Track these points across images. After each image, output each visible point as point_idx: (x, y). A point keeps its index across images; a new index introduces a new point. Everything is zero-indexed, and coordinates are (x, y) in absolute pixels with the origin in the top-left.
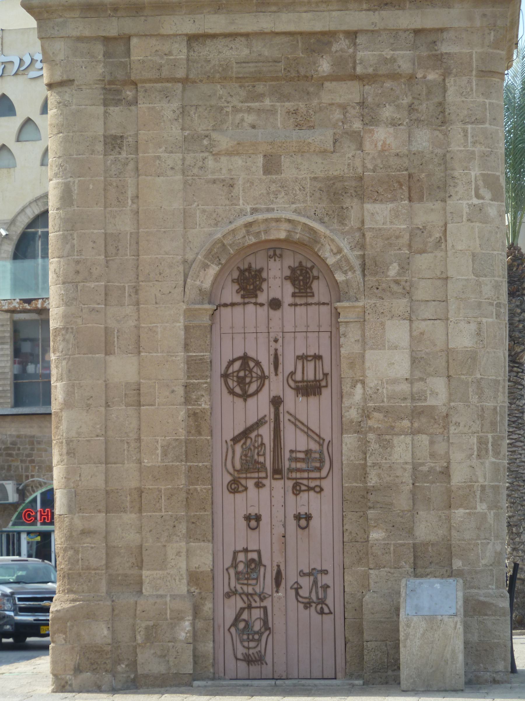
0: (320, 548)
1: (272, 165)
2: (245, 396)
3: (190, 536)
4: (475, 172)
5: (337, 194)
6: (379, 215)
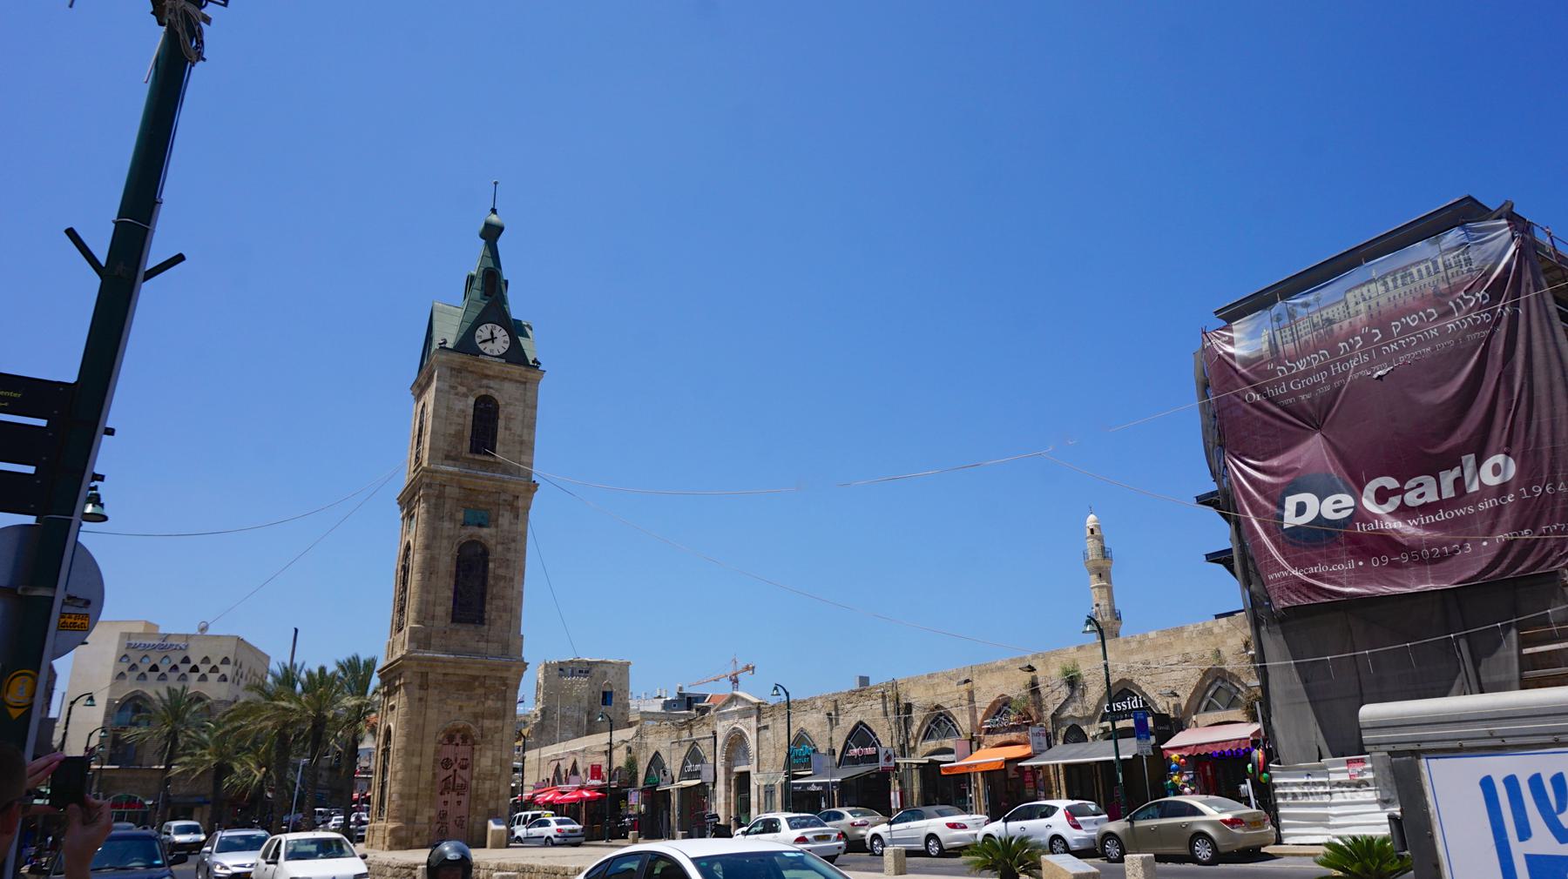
0: (463, 810)
1: (461, 708)
6: (487, 723)
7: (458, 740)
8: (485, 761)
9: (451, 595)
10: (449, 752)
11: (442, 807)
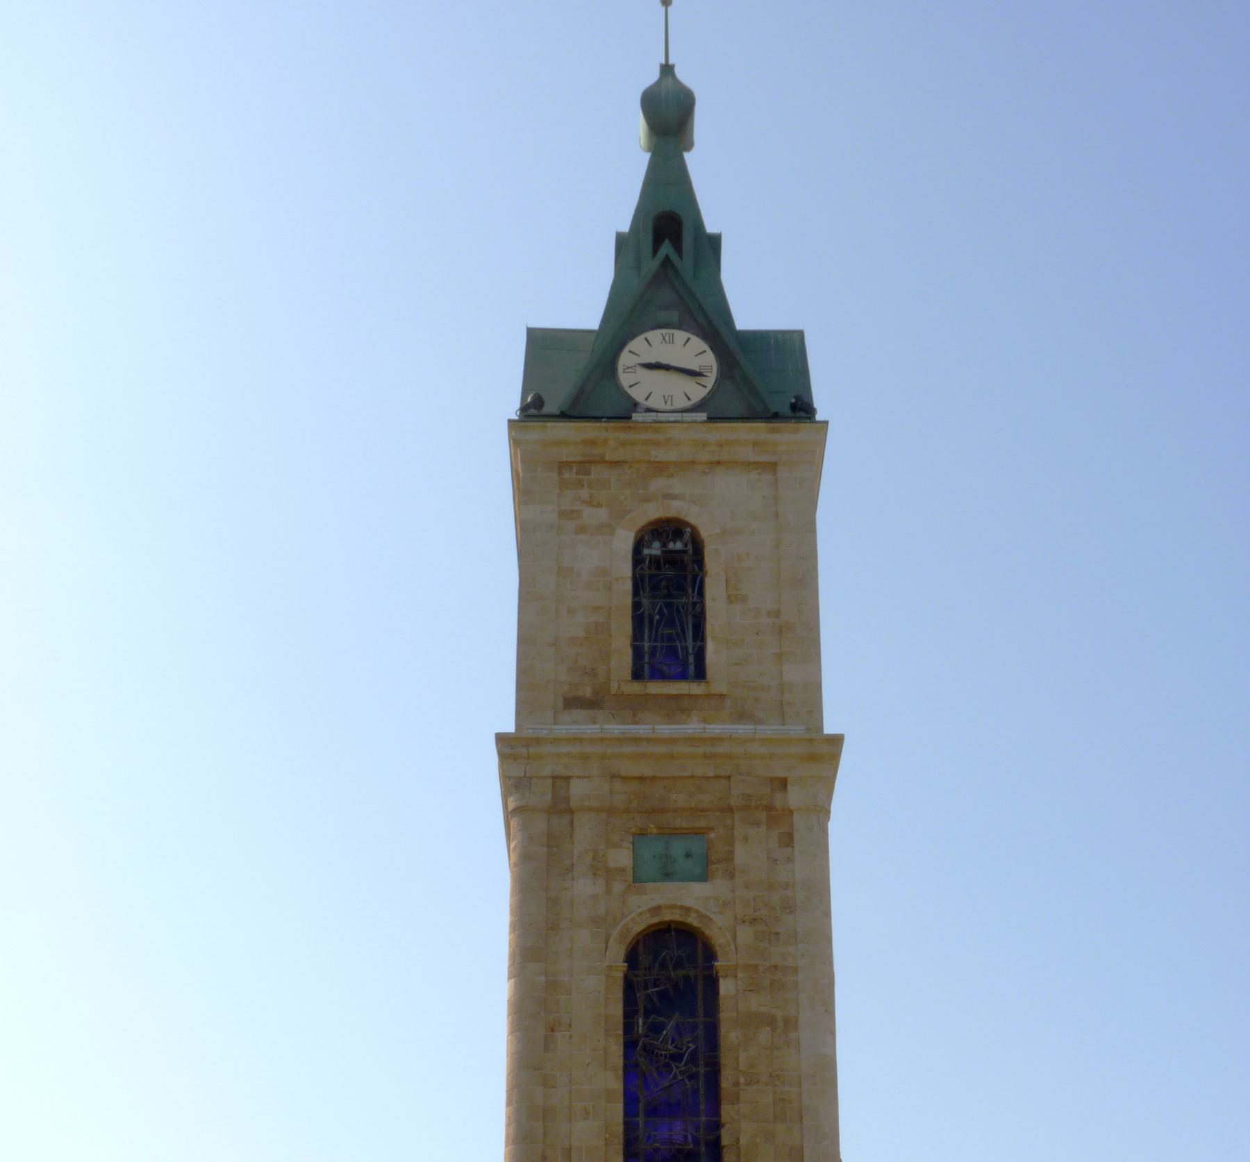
9: (617, 1085)
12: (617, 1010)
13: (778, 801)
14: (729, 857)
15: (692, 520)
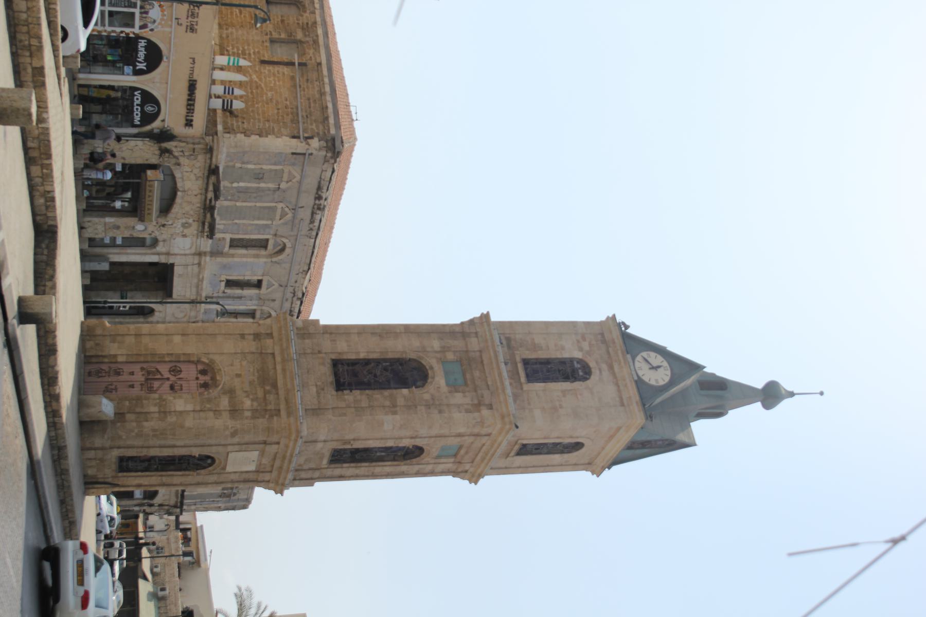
1: (238, 376)
2: (170, 371)
3: (128, 355)
4: (238, 426)
5: (231, 392)
6: (225, 402)
7: (203, 379)
8: (180, 404)
9: (362, 356)
10: (189, 372)
11: (127, 369)
12: (390, 356)
13: (482, 408)
14: (457, 391)
15: (592, 377)
